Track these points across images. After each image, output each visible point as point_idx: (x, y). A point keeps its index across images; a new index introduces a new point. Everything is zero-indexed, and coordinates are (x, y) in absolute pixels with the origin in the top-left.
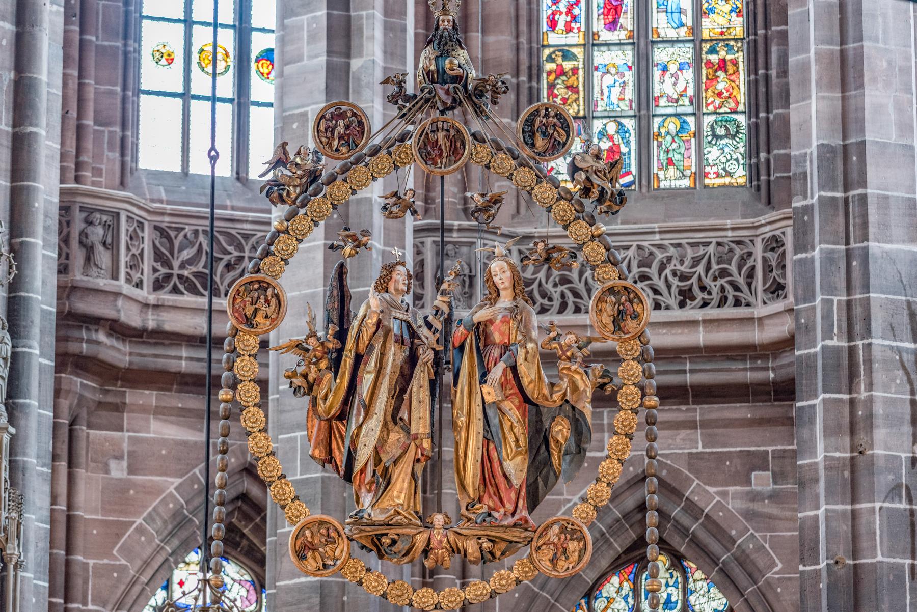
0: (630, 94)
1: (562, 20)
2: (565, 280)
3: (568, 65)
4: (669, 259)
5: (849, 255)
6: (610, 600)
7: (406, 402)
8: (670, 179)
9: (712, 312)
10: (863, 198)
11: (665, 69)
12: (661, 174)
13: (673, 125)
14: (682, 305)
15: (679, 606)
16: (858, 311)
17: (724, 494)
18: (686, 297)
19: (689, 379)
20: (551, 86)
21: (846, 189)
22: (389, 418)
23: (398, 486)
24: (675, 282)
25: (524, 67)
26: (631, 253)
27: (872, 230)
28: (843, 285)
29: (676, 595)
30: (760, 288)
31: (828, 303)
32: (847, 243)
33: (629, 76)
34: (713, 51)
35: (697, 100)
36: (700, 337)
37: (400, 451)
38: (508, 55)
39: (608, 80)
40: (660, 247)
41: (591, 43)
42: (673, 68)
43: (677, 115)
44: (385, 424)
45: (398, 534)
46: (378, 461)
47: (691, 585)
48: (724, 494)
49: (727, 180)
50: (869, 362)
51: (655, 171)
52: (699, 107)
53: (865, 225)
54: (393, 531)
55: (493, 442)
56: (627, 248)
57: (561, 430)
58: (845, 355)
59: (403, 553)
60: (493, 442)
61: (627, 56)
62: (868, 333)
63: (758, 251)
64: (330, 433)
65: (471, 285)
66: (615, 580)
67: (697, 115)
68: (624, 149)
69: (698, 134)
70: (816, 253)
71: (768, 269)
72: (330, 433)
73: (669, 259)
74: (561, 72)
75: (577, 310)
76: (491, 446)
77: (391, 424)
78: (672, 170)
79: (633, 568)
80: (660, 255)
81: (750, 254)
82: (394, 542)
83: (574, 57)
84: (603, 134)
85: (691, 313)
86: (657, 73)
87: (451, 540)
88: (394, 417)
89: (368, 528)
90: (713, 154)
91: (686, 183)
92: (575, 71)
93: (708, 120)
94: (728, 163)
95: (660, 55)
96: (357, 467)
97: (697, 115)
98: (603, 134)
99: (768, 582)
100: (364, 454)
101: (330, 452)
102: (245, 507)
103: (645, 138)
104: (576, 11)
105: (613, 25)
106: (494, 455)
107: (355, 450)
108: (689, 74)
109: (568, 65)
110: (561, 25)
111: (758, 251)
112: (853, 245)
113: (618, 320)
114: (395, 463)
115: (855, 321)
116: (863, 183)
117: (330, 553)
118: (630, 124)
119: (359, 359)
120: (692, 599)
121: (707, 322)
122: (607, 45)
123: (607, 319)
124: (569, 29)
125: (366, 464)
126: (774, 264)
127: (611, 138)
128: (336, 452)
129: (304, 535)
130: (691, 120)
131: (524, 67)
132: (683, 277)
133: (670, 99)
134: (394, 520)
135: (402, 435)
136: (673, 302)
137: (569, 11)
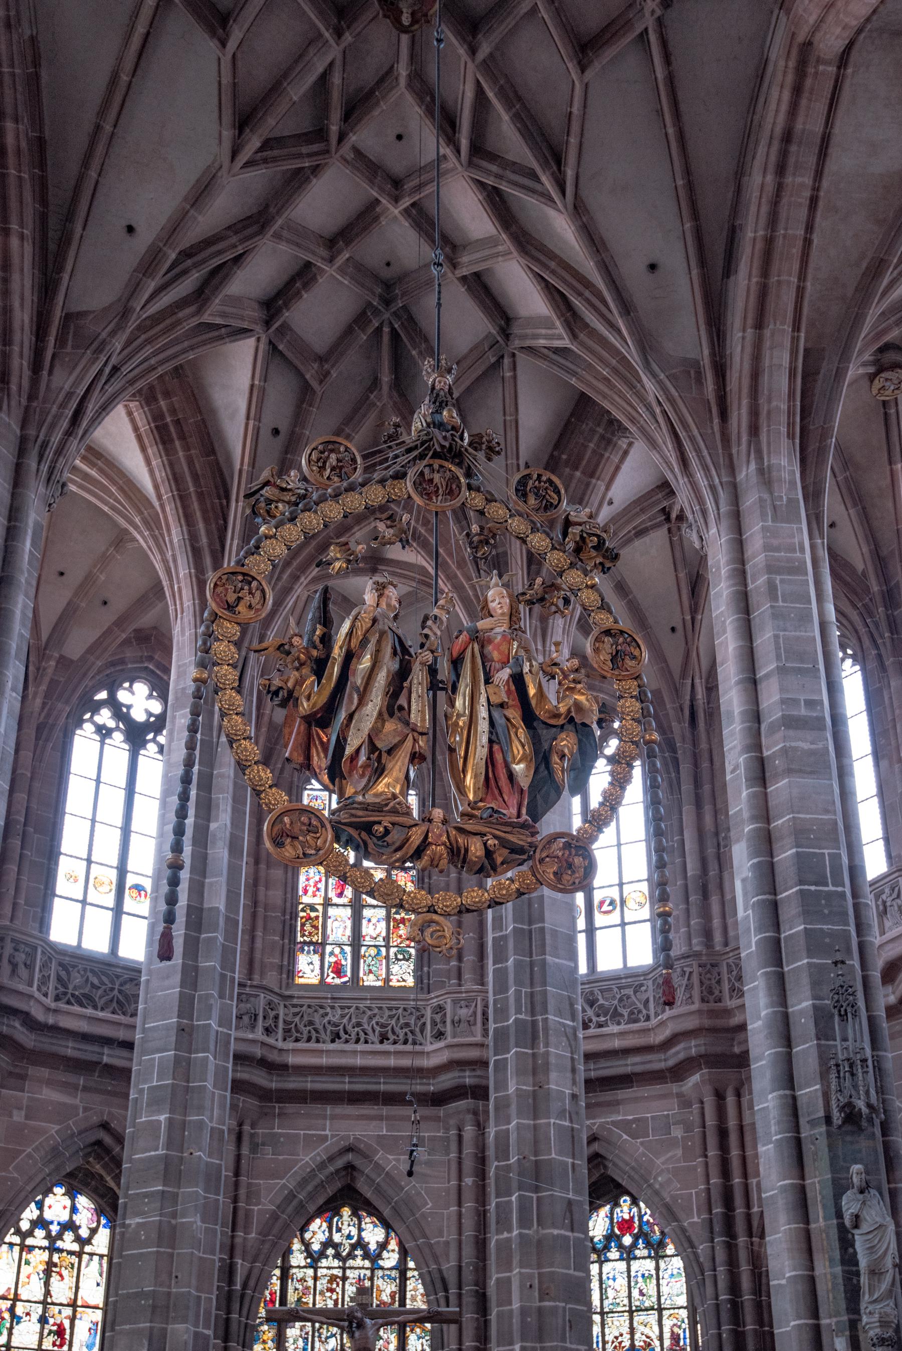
0: (348, 932)
1: (311, 890)
2: (311, 1023)
3: (313, 914)
4: (375, 1015)
5: (532, 964)
6: (314, 1233)
7: (405, 691)
8: (370, 981)
9: (400, 1047)
10: (542, 930)
11: (369, 921)
12: (365, 978)
13: (373, 951)
14: (381, 1042)
15: (355, 1238)
16: (538, 998)
17: (398, 1160)
18: (383, 1038)
19: (382, 1087)
20: (303, 925)
21: (530, 924)
22: (384, 709)
23: (395, 774)
24: (378, 1029)
25: (288, 911)
26: (352, 1010)
27: (548, 949)
28: (528, 982)
29: (354, 1232)
30: (429, 1035)
31: (518, 992)
32: (531, 957)
33: (349, 924)
34: (397, 913)
35: (387, 939)
36: (392, 1062)
37: (398, 739)
38: (279, 902)
39: (336, 924)
40: (370, 1009)
41: (327, 903)
42: (374, 920)
43: (375, 946)
44: (380, 714)
45: (393, 824)
46: (373, 748)
47: (363, 1226)
48: (398, 1160)
49: (403, 984)
50: (546, 1029)
51: (361, 975)
52: (388, 942)
53: (543, 945)
54: (388, 818)
55: (499, 743)
56: (349, 1008)
57: (566, 742)
58: (529, 1025)
59: (397, 844)
60: (499, 743)
61: (348, 912)
62: (545, 1011)
63: (428, 1013)
64: (309, 739)
65: (255, 1020)
66: (318, 1221)
67: (388, 947)
68: (343, 962)
69: (387, 957)
70: (511, 962)
71: (434, 1023)
72: (309, 739)
73: (375, 1015)
74: (309, 918)
75: (318, 1041)
76: (496, 747)
77: (386, 716)
78: (371, 976)
79: (329, 1214)
80: (369, 1013)
81: (423, 1016)
82: (387, 832)
83: (317, 910)
84: (332, 953)
85: (387, 1047)
86: (364, 922)
87: (452, 839)
88: (394, 707)
89: (360, 813)
90: (395, 969)
91: (379, 984)
92: (317, 917)
93: (393, 950)
94: (403, 974)
95: (367, 913)
96: (349, 751)
97: (388, 947)
98: (332, 953)
99: (423, 1216)
100: (353, 742)
101: (308, 757)
102: (99, 1151)
103: (356, 957)
104: (319, 886)
105: (340, 895)
106: (499, 757)
107: (345, 740)
108: (383, 924)
109: (313, 914)
110: (310, 893)
111: (428, 1013)
112: (535, 958)
113: (616, 658)
114: (390, 752)
115: (537, 1004)
116: (542, 920)
117: (311, 842)
118: (348, 949)
119: (349, 657)
120: (363, 1234)
121: (397, 1053)
122: (337, 905)
123: (605, 656)
124: (314, 896)
125: (358, 751)
126: (438, 1020)
127: (336, 956)
128: (316, 758)
129: (282, 822)
130: (383, 950)
131: (288, 911)
132: (383, 1026)
133: (371, 937)
134: (391, 804)
135: (400, 726)
136: (376, 1039)
137: (316, 883)
